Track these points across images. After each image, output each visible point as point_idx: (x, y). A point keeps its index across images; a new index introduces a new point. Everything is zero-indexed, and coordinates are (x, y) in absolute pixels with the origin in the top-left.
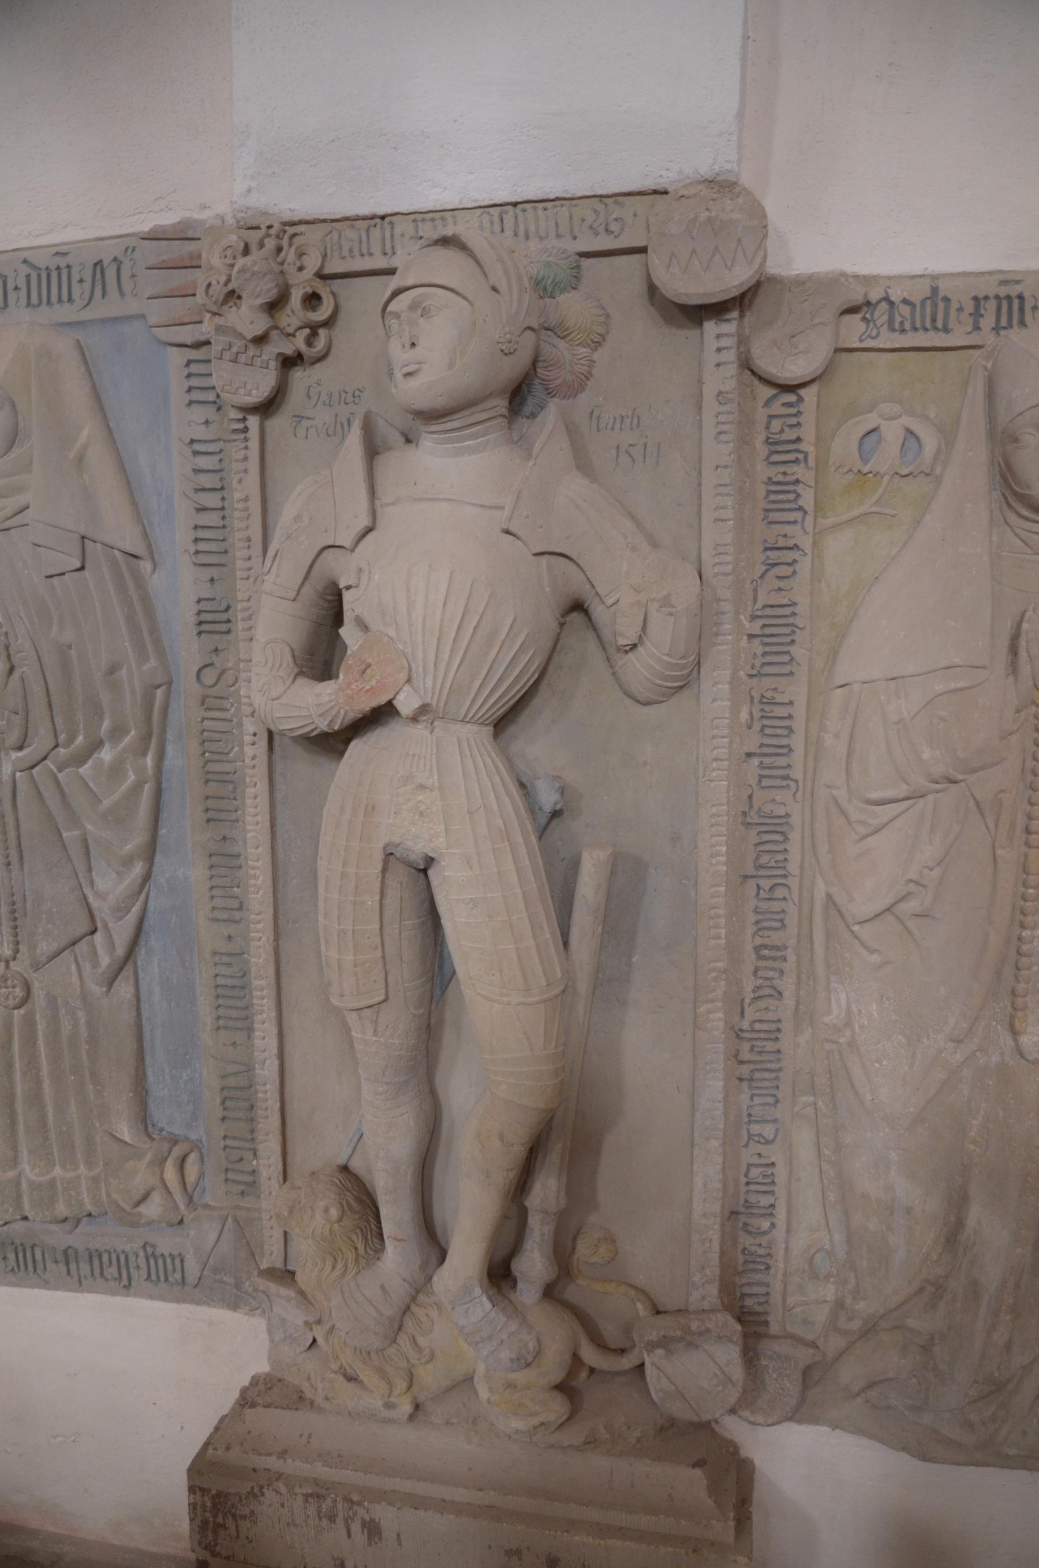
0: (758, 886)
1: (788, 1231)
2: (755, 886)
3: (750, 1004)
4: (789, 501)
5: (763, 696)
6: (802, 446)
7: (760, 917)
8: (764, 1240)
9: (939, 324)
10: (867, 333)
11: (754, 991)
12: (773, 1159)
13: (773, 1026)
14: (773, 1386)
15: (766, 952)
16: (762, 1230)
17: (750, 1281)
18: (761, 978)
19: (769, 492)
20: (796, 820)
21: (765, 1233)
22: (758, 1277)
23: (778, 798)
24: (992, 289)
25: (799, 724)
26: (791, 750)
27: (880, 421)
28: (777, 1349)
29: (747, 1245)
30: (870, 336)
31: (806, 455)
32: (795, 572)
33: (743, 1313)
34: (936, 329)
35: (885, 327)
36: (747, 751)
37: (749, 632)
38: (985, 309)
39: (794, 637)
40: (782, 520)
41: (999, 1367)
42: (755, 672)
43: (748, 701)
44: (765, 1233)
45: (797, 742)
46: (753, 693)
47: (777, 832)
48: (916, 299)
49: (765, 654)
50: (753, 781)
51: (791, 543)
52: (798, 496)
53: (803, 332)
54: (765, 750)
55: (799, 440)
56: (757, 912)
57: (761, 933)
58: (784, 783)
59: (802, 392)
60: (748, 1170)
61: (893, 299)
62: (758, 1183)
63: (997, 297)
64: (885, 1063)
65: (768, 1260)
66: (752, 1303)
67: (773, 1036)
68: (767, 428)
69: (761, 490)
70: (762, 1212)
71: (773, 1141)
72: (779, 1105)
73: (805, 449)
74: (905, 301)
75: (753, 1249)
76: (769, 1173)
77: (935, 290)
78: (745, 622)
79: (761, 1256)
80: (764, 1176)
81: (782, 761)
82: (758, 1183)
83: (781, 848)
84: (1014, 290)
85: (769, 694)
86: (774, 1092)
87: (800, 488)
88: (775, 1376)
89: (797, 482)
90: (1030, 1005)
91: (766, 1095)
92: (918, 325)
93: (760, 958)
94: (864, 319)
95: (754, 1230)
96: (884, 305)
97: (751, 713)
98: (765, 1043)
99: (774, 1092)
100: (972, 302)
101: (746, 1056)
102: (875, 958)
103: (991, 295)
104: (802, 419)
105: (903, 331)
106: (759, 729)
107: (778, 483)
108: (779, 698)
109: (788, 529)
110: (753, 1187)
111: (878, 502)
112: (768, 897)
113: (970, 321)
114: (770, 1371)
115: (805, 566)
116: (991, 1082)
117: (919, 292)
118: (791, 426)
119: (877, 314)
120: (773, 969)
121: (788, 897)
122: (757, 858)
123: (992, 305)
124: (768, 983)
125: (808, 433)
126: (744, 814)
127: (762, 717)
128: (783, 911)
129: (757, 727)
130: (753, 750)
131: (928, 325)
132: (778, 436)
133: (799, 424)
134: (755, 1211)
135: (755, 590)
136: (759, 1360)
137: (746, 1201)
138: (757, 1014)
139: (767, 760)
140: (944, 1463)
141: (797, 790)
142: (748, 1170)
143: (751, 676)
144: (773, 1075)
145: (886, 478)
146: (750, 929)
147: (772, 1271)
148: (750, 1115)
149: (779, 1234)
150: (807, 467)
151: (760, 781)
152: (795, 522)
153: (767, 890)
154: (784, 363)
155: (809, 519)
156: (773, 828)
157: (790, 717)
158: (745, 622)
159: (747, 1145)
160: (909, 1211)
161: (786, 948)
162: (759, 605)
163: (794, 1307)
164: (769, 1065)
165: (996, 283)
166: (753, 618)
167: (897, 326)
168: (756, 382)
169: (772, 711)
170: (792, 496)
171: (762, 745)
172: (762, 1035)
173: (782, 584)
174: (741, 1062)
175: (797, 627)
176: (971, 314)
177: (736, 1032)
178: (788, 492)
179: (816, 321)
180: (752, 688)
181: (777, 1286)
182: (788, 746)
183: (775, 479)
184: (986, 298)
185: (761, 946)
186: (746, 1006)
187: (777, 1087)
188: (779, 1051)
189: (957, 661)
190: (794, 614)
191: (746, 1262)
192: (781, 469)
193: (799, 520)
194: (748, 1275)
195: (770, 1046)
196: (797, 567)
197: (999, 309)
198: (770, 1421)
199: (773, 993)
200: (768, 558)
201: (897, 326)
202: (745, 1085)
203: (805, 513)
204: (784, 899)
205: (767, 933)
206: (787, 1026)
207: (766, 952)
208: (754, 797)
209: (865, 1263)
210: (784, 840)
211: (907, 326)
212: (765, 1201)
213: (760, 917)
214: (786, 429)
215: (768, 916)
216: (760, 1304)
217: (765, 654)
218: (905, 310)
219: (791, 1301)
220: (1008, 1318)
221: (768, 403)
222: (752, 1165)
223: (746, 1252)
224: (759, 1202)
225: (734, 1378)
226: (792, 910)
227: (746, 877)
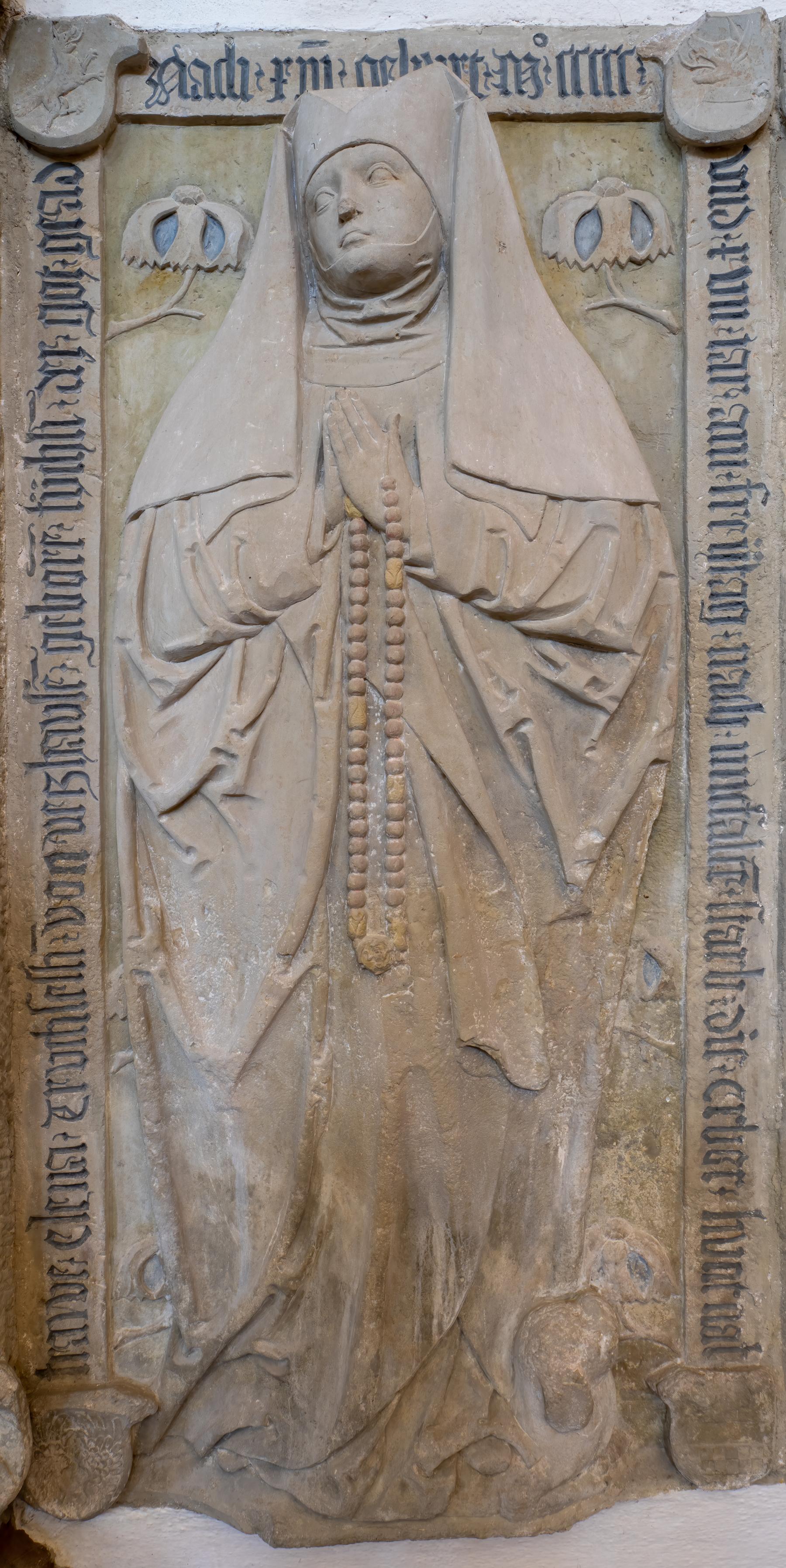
0: (48, 776)
1: (110, 1235)
2: (44, 776)
3: (43, 932)
4: (71, 297)
5: (45, 535)
6: (84, 230)
7: (52, 816)
8: (76, 1253)
9: (237, 90)
10: (155, 99)
11: (47, 914)
12: (83, 1140)
13: (74, 960)
14: (90, 1460)
15: (62, 863)
16: (74, 1238)
17: (64, 1311)
18: (57, 896)
19: (46, 285)
20: (92, 689)
21: (78, 1242)
22: (72, 1305)
23: (69, 663)
24: (294, 50)
25: (91, 568)
26: (83, 602)
27: (177, 204)
28: (89, 1405)
29: (55, 1262)
30: (158, 102)
31: (89, 240)
32: (80, 383)
33: (54, 1358)
34: (235, 96)
35: (176, 91)
36: (28, 604)
37: (25, 455)
38: (288, 74)
39: (83, 462)
40: (62, 318)
41: (365, 1398)
42: (35, 505)
43: (28, 540)
44: (78, 1242)
45: (90, 591)
46: (33, 530)
47: (72, 706)
48: (210, 61)
49: (46, 482)
50: (38, 642)
51: (74, 346)
52: (82, 291)
53: (74, 89)
54: (51, 602)
55: (79, 223)
56: (49, 811)
57: (53, 837)
58: (76, 644)
59: (82, 165)
60: (51, 1157)
61: (183, 60)
62: (66, 1174)
63: (300, 60)
64: (211, 995)
65: (83, 1280)
66: (65, 1344)
67: (74, 973)
68: (41, 207)
69: (37, 282)
70: (73, 1213)
71: (81, 1114)
72: (88, 1065)
73: (88, 234)
74: (197, 63)
75: (63, 1266)
76: (79, 1159)
77: (230, 51)
78: (20, 443)
79: (73, 1275)
80: (72, 1163)
81: (72, 616)
82: (66, 1174)
83: (74, 725)
84: (319, 53)
85: (53, 532)
86: (80, 1047)
87: (83, 281)
88: (92, 1445)
89: (80, 273)
90: (369, 901)
91: (70, 1053)
92: (213, 90)
93: (55, 870)
94: (150, 81)
95: (64, 1240)
96: (173, 67)
97: (32, 556)
98: (65, 983)
99: (80, 1047)
100: (273, 66)
101: (41, 1001)
102: (191, 860)
103: (294, 58)
104: (82, 197)
105: (197, 98)
106: (42, 575)
107: (57, 274)
108: (66, 537)
109: (71, 330)
110: (58, 1181)
111: (179, 301)
112: (60, 789)
113: (272, 87)
114: (86, 1439)
115: (92, 375)
116: (334, 1008)
117: (213, 52)
118: (69, 206)
119: (165, 77)
120: (73, 884)
121: (86, 788)
122: (45, 740)
123: (295, 68)
124: (65, 903)
125: (90, 214)
126: (27, 684)
127: (46, 561)
128: (81, 807)
129: (40, 572)
130: (34, 603)
131: (225, 91)
132: (55, 217)
133: (78, 204)
134: (63, 1213)
135: (32, 403)
136: (68, 1425)
137: (50, 1201)
138: (53, 944)
139: (53, 615)
140: (302, 1546)
141: (92, 651)
142: (51, 1157)
143: (31, 509)
144: (78, 1025)
145: (189, 273)
146: (40, 833)
147: (89, 1295)
148: (50, 1081)
149: (97, 1242)
150: (91, 255)
151: (45, 642)
152: (78, 322)
153: (59, 781)
154: (51, 123)
155: (96, 319)
156: (63, 701)
157: (80, 560)
158: (20, 443)
159: (47, 1124)
160: (251, 1191)
161: (88, 855)
162: (38, 422)
163: (122, 1342)
164: (72, 1013)
165: (299, 44)
166: (32, 437)
167: (189, 91)
168: (24, 151)
169: (58, 553)
170: (74, 291)
171: (47, 597)
172: (61, 972)
173: (65, 396)
174: (36, 1011)
175: (85, 449)
176: (273, 80)
177: (27, 972)
178: (70, 285)
179: (88, 75)
180: (32, 525)
181: (98, 1316)
182: (78, 596)
183: (52, 269)
184: (288, 61)
185: (54, 854)
186: (38, 935)
187: (84, 1040)
188: (83, 992)
189: (257, 469)
190: (81, 433)
191: (55, 1286)
192: (60, 256)
193: (84, 319)
194: (59, 1304)
195: (72, 986)
196: (83, 376)
197: (303, 76)
198: (84, 1514)
199: (73, 915)
200: (46, 364)
201: (189, 91)
202: (42, 1041)
203: (92, 311)
204: (82, 791)
205: (62, 837)
206: (92, 958)
207: (62, 863)
208: (39, 662)
209: (206, 1270)
210: (80, 716)
211: (201, 91)
212: (75, 1197)
213: (52, 816)
214: (63, 209)
215: (62, 815)
216: (77, 1342)
217: (46, 482)
218: (198, 73)
219: (120, 1332)
220: (372, 1326)
221: (41, 177)
222: (57, 1149)
223: (55, 1272)
224: (67, 1200)
225: (11, 1463)
226: (92, 805)
227: (32, 765)
